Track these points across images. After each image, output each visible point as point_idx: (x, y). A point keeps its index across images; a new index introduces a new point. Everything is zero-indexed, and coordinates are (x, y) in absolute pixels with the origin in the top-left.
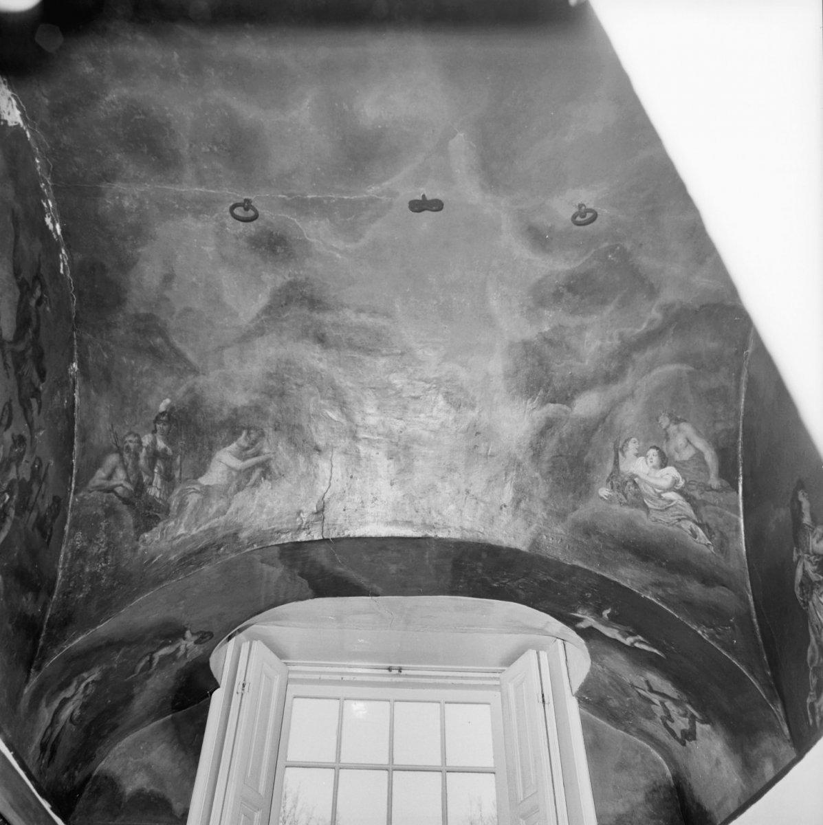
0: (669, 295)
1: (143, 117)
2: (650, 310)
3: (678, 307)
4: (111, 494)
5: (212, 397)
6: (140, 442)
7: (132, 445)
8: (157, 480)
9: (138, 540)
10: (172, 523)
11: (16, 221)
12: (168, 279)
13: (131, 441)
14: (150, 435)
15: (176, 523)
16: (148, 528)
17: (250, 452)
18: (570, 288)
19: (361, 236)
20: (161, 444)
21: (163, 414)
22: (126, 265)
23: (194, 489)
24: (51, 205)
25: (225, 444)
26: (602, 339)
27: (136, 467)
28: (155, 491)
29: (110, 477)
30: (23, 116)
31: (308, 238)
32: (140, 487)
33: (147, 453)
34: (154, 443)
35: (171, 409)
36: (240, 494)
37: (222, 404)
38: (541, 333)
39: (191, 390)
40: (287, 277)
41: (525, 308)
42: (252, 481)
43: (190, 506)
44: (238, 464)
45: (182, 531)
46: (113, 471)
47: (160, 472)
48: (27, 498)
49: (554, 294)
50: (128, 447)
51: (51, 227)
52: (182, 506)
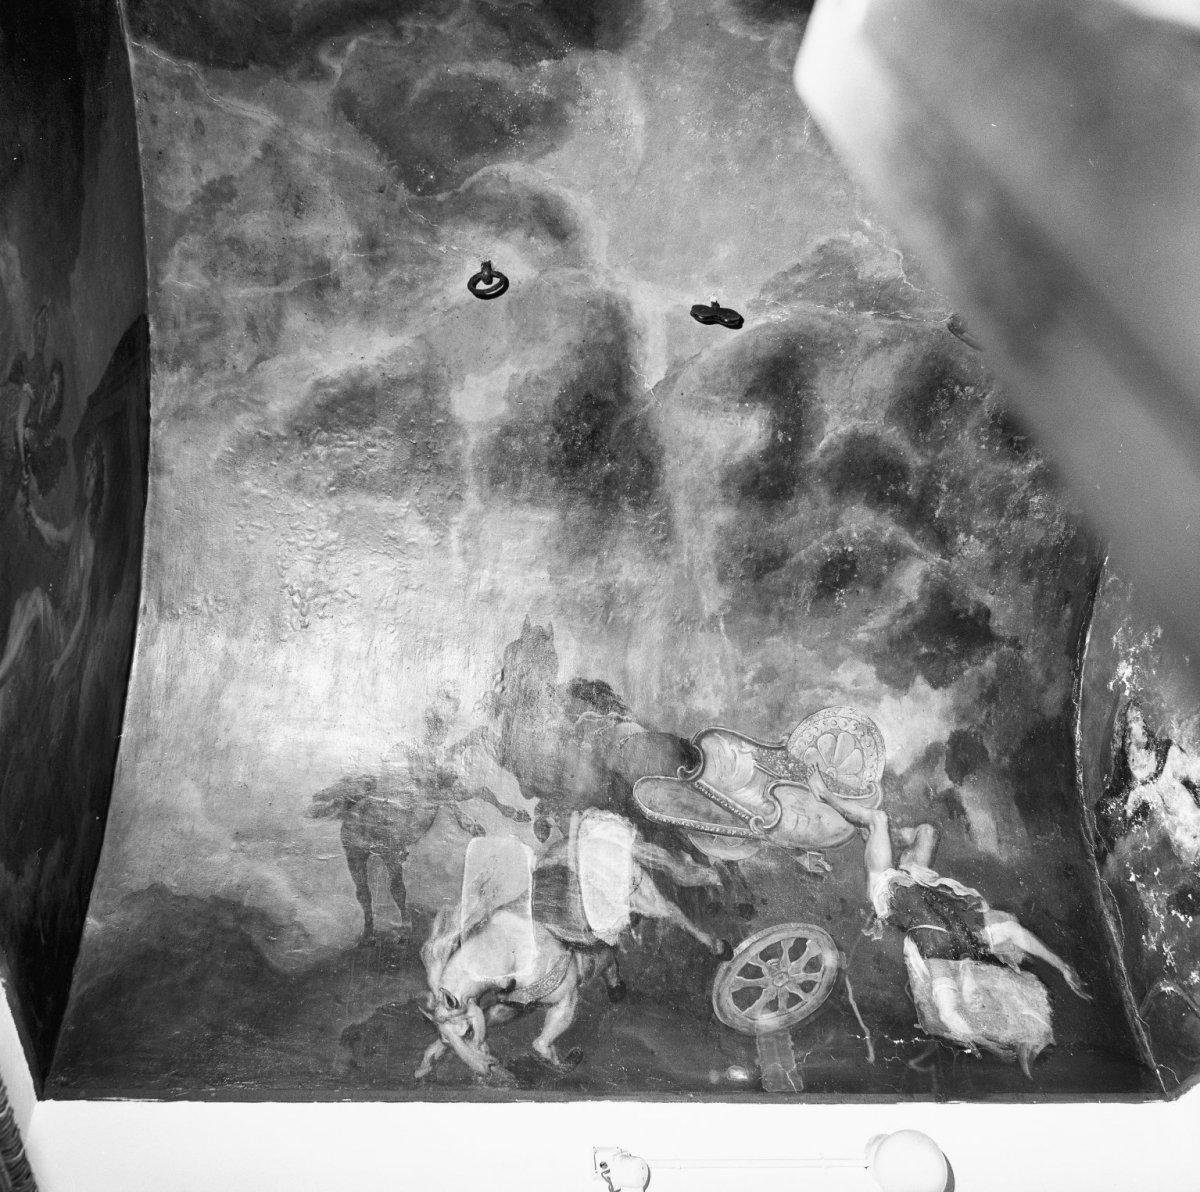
0: (317, 97)
2: (346, 73)
3: (293, 72)
18: (500, 131)
19: (821, 249)
26: (434, 32)
38: (555, 58)
41: (582, 102)
49: (528, 122)
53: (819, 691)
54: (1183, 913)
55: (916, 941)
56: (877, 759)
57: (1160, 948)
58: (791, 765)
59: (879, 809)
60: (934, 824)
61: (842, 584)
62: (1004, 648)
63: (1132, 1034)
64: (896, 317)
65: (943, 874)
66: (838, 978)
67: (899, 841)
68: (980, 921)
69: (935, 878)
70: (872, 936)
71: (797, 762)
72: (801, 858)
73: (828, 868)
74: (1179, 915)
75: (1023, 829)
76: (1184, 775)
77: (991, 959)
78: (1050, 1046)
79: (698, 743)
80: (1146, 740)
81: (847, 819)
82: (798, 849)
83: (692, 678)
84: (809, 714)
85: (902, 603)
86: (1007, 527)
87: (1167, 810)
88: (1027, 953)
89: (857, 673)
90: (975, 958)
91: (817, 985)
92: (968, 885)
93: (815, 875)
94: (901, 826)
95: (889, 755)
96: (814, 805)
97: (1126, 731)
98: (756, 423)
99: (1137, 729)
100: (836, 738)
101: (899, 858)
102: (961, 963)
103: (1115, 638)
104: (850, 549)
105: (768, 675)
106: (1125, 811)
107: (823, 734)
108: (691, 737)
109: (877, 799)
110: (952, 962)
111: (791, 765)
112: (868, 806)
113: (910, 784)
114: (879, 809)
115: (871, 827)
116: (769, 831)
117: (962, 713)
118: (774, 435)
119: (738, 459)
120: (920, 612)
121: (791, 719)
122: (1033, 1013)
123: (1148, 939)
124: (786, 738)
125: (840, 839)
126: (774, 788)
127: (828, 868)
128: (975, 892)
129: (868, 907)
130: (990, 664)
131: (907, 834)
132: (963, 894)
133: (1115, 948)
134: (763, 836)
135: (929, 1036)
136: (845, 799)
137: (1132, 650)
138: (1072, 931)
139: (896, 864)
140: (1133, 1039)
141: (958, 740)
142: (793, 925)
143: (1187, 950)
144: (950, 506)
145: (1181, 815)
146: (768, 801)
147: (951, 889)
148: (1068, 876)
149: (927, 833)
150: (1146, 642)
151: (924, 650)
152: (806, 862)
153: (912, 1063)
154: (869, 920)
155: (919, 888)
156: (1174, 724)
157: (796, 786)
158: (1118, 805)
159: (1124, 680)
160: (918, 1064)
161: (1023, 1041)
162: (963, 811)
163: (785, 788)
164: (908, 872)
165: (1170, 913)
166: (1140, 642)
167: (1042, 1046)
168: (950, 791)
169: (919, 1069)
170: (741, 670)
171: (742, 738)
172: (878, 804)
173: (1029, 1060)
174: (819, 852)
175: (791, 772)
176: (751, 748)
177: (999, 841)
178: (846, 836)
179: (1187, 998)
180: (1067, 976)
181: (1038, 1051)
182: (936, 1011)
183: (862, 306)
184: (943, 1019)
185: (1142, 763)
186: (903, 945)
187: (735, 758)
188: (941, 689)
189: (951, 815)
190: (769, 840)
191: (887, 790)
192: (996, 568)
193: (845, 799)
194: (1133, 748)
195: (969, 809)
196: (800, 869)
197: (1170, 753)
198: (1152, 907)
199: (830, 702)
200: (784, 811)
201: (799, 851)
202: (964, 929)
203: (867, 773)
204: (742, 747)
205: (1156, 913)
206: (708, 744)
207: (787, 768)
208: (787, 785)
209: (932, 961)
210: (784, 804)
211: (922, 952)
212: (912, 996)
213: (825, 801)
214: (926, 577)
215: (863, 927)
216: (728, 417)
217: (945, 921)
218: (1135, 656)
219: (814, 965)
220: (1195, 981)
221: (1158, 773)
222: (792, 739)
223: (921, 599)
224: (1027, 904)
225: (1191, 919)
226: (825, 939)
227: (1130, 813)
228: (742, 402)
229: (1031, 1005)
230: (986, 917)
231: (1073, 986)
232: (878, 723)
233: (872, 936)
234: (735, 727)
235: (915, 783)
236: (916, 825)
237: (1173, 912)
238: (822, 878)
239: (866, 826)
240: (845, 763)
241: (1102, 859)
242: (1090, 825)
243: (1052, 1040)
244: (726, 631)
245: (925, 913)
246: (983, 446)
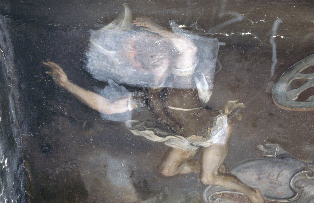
55: (199, 99)
59: (207, 186)
60: (162, 176)
63: (11, 37)
65: (162, 144)
66: (280, 75)
67: (194, 164)
68: (135, 114)
69: (168, 141)
70: (237, 103)
72: (282, 153)
73: (261, 147)
75: (82, 174)
77: (130, 88)
78: (95, 29)
81: (236, 178)
82: (283, 158)
90: (147, 90)
91: (300, 71)
92: (140, 138)
93: (274, 142)
94: (190, 175)
101: (197, 154)
102: (162, 86)
109: (208, 191)
110: (170, 86)
115: (216, 173)
116: (304, 169)
122: (106, 52)
125: (245, 165)
127: (261, 147)
128: (135, 133)
129: (232, 120)
131: (186, 169)
132: (147, 132)
133: (14, 99)
134: (309, 165)
135: (214, 37)
136: (235, 191)
138: (52, 109)
139: (201, 151)
140: (11, 32)
142: (304, 110)
146: (300, 188)
147: (156, 134)
148: (49, 146)
152: (278, 149)
153: (240, 17)
154: (236, 114)
155: (185, 135)
157: (274, 198)
160: (235, 17)
161: (123, 32)
162: (135, 185)
163: (284, 197)
164: (192, 145)
167: (106, 28)
169: (231, 13)
173: (123, 17)
174: (265, 157)
177: (105, 166)
178: (239, 168)
180: (64, 79)
181: (111, 25)
182: (199, 55)
184: (195, 49)
186: (212, 98)
189: (146, 183)
190: (304, 163)
191: (199, 198)
193: (235, 191)
195: (130, 188)
196: (284, 146)
200: (288, 182)
201: (282, 157)
202: (152, 109)
209: (189, 87)
210: (287, 187)
211: (196, 92)
212: (217, 64)
213: (253, 190)
215: (242, 109)
217: (167, 113)
219: (297, 84)
224: (90, 126)
226: (279, 101)
229: (106, 57)
233: (237, 103)
236: (177, 176)
238: (268, 140)
239: (220, 174)
243: (93, 33)
245: (183, 118)
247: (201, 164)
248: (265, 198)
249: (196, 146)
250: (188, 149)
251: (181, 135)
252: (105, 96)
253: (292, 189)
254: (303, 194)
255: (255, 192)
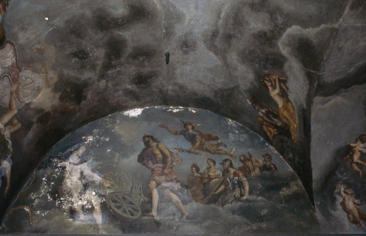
1: (136, 80)
4: (276, 136)
5: (249, 85)
6: (261, 117)
7: (261, 120)
8: (276, 120)
9: (293, 141)
10: (292, 127)
11: (162, 126)
12: (200, 82)
13: (260, 119)
14: (259, 112)
15: (292, 125)
16: (291, 136)
17: (274, 83)
20: (263, 111)
21: (252, 104)
22: (195, 94)
23: (282, 111)
24: (172, 107)
25: (268, 90)
27: (269, 123)
28: (279, 124)
29: (271, 133)
30: (141, 108)
31: (184, 33)
32: (276, 126)
33: (265, 116)
34: (262, 113)
35: (251, 101)
36: (289, 97)
37: (252, 83)
39: (245, 91)
40: (201, 43)
42: (286, 90)
43: (288, 117)
44: (277, 91)
45: (295, 126)
46: (269, 131)
47: (273, 117)
48: (248, 169)
50: (262, 121)
51: (178, 110)
52: (286, 119)
53: (43, 70)
54: (50, 197)
56: (32, 98)
57: (35, 199)
58: (16, 76)
60: (22, 126)
61: (79, 58)
62: (77, 108)
64: (164, 38)
65: (11, 139)
68: (5, 158)
69: (8, 138)
71: (18, 77)
74: (49, 196)
76: (83, 170)
79: (7, 42)
80: (81, 156)
81: (10, 103)
83: (28, 28)
84: (35, 71)
85: (80, 77)
86: (111, 90)
87: (70, 173)
88: (6, 175)
89: (53, 76)
94: (17, 118)
95: (34, 101)
96: (8, 91)
97: (77, 149)
98: (122, 12)
99: (81, 151)
100: (32, 83)
103: (95, 130)
104: (91, 55)
105: (41, 51)
106: (58, 164)
107: (31, 79)
108: (8, 39)
111: (16, 76)
112: (17, 106)
113: (29, 111)
114: (18, 109)
115: (11, 111)
117: (55, 109)
118: (120, 18)
119: (109, 11)
120: (79, 82)
121: (30, 67)
123: (33, 195)
124: (24, 69)
125: (3, 106)
126: (6, 76)
128: (12, 150)
130: (72, 107)
136: (15, 98)
137: (97, 137)
139: (6, 125)
141: (48, 114)
143: (43, 205)
144: (112, 74)
145: (73, 177)
147: (8, 144)
149: (19, 126)
150: (102, 138)
151: (68, 90)
156: (92, 159)
158: (57, 161)
159: (88, 140)
163: (8, 79)
164: (5, 130)
165: (47, 194)
166: (101, 136)
168: (34, 122)
170: (39, 43)
171: (16, 55)
172: (19, 108)
175: (14, 77)
176: (14, 60)
179: (30, 215)
180: (7, 188)
183: (166, 28)
185: (74, 158)
187: (9, 58)
188: (60, 101)
192: (98, 93)
193: (15, 98)
194: (75, 154)
195: (31, 130)
197: (84, 164)
198: (43, 189)
199: (41, 74)
203: (26, 98)
204: (13, 58)
205: (42, 191)
206: (8, 46)
207: (15, 75)
208: (9, 79)
210: (3, 82)
213: (11, 93)
214: (90, 78)
216: (122, 2)
218: (96, 138)
220: (38, 213)
221: (76, 164)
222: (24, 71)
223: (83, 81)
225: (51, 200)
227: (59, 165)
228: (128, 5)
230: (7, 158)
231: (6, 192)
232: (42, 91)
234: (18, 51)
235: (30, 112)
237: (48, 195)
239: (11, 109)
240: (25, 91)
241: (40, 168)
242: (45, 159)
244: (50, 31)
246: (132, 74)
247: (11, 120)
248: (12, 85)
249: (5, 128)
250: (8, 129)
251: (4, 137)
252: (5, 173)
253: (3, 79)
254: (3, 73)
255: (11, 91)
